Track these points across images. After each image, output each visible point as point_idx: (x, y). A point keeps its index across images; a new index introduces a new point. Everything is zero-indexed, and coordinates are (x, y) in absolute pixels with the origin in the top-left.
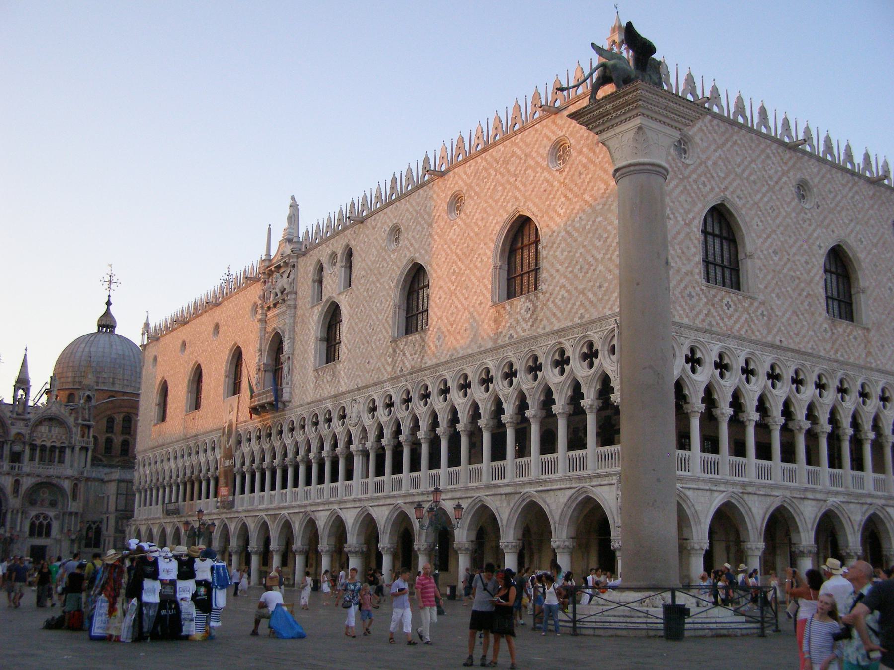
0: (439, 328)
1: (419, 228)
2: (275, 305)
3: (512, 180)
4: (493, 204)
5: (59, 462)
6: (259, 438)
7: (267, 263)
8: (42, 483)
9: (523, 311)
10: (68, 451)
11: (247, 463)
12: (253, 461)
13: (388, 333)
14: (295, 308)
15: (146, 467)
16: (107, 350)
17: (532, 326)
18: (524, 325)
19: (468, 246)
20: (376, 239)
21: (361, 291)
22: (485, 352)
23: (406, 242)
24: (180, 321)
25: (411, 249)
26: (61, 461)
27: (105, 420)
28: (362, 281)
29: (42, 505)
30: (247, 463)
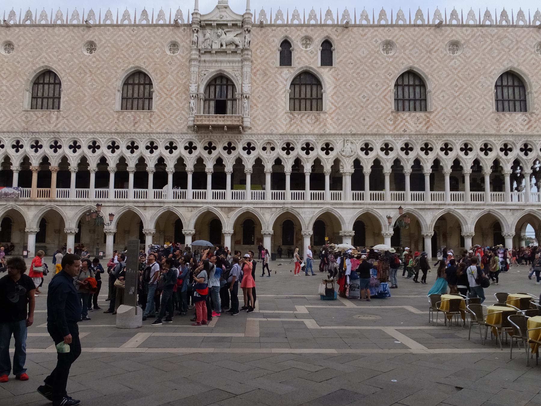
0: (444, 114)
1: (416, 50)
3: (507, 50)
4: (491, 58)
6: (190, 148)
9: (520, 120)
13: (387, 105)
17: (528, 129)
18: (522, 127)
19: (469, 74)
20: (366, 44)
21: (351, 72)
22: (490, 135)
23: (402, 54)
25: (410, 61)
28: (351, 66)
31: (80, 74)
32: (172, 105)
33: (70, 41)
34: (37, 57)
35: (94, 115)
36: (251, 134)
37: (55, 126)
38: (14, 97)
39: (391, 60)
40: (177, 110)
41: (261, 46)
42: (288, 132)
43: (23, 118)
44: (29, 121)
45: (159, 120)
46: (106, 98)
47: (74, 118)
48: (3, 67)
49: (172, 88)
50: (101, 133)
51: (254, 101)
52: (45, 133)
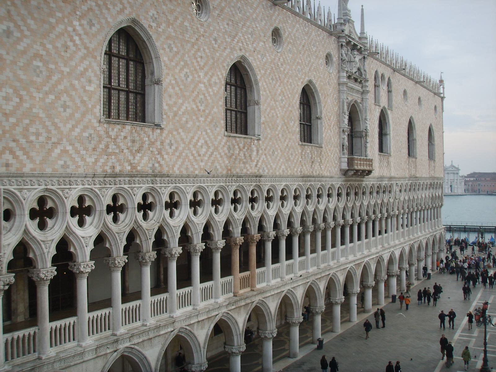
31: (272, 79)
32: (331, 139)
33: (262, 21)
34: (234, 37)
35: (285, 149)
37: (256, 166)
38: (213, 107)
39: (406, 108)
40: (334, 147)
43: (225, 149)
44: (233, 154)
45: (325, 159)
46: (293, 122)
47: (271, 153)
48: (200, 43)
49: (331, 117)
50: (293, 176)
52: (249, 176)
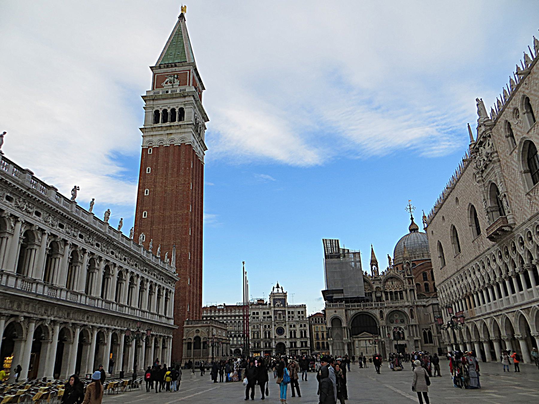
2: (485, 168)
5: (401, 299)
6: (501, 257)
7: (473, 146)
8: (394, 311)
10: (404, 293)
11: (498, 276)
12: (501, 274)
14: (499, 161)
15: (443, 293)
16: (416, 241)
24: (439, 207)
26: (402, 298)
27: (422, 274)
29: (397, 323)
30: (498, 276)
36: (516, 230)
41: (499, 143)
42: (532, 214)
50: (472, 261)
51: (510, 196)
